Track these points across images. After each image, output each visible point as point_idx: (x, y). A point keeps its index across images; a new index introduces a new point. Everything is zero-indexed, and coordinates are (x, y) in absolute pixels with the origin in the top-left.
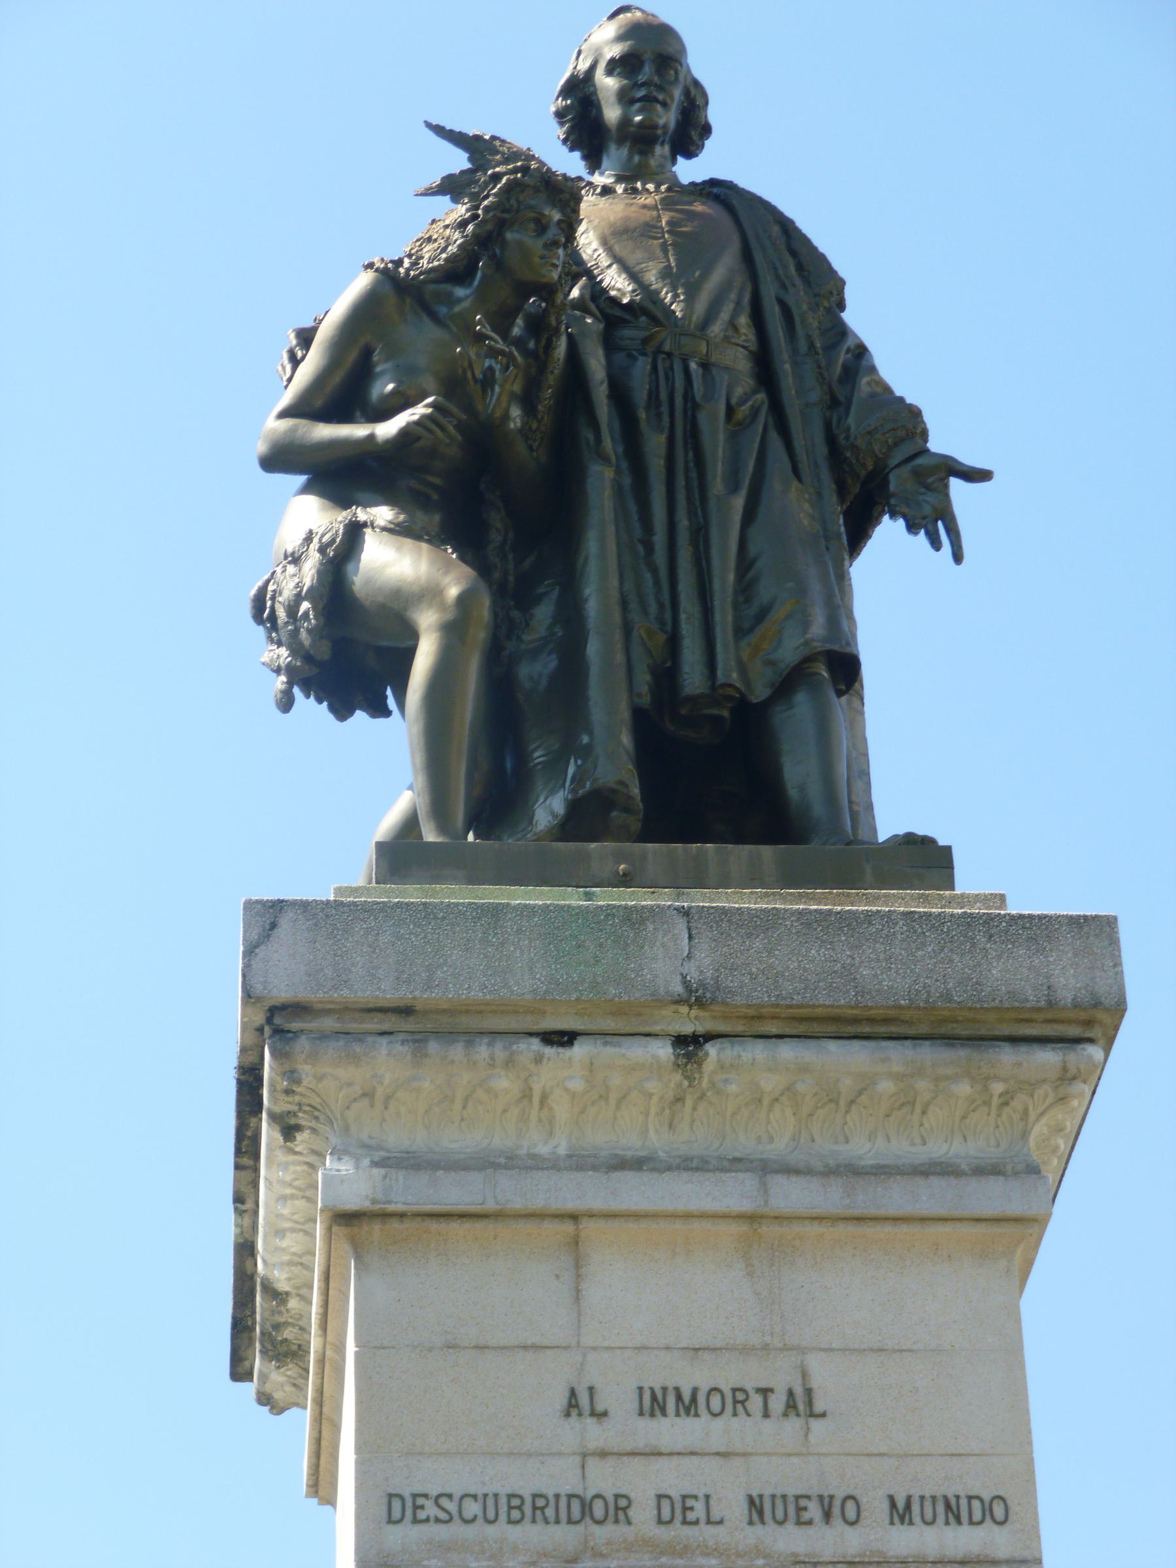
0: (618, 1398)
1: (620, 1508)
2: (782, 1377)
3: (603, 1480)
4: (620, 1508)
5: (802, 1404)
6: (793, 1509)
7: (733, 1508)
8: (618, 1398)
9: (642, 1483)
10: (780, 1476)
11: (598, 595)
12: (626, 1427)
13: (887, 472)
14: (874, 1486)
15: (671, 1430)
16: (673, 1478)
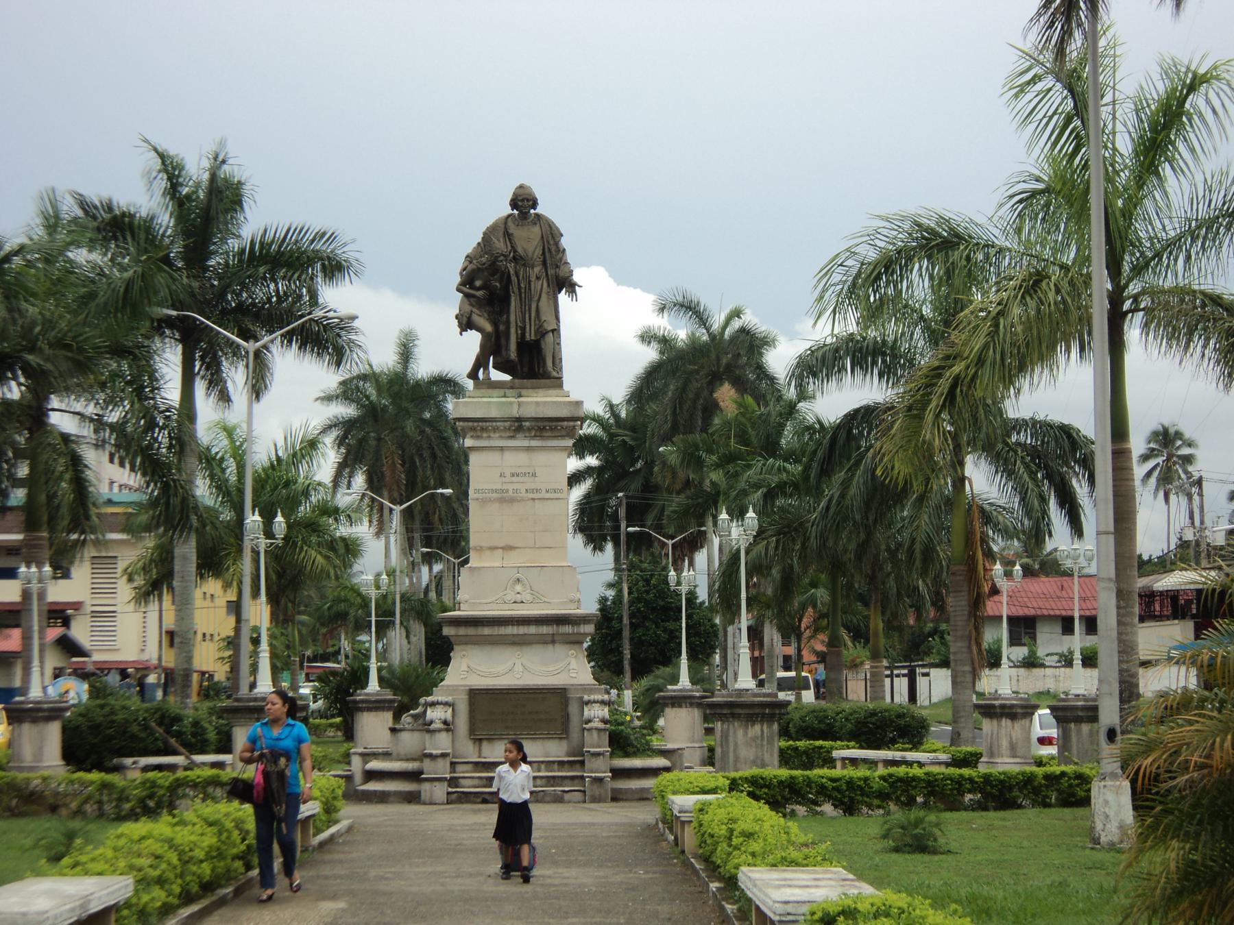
0: (508, 475)
1: (507, 491)
2: (531, 471)
3: (505, 487)
4: (507, 491)
5: (534, 475)
6: (532, 491)
7: (523, 491)
8: (508, 475)
9: (510, 487)
10: (533, 486)
11: (512, 318)
12: (509, 479)
13: (565, 283)
14: (544, 487)
15: (515, 479)
16: (516, 486)
